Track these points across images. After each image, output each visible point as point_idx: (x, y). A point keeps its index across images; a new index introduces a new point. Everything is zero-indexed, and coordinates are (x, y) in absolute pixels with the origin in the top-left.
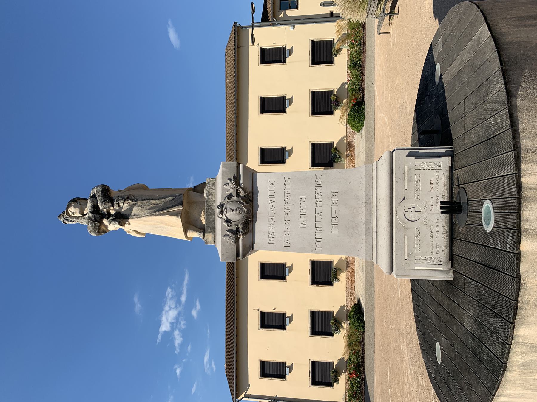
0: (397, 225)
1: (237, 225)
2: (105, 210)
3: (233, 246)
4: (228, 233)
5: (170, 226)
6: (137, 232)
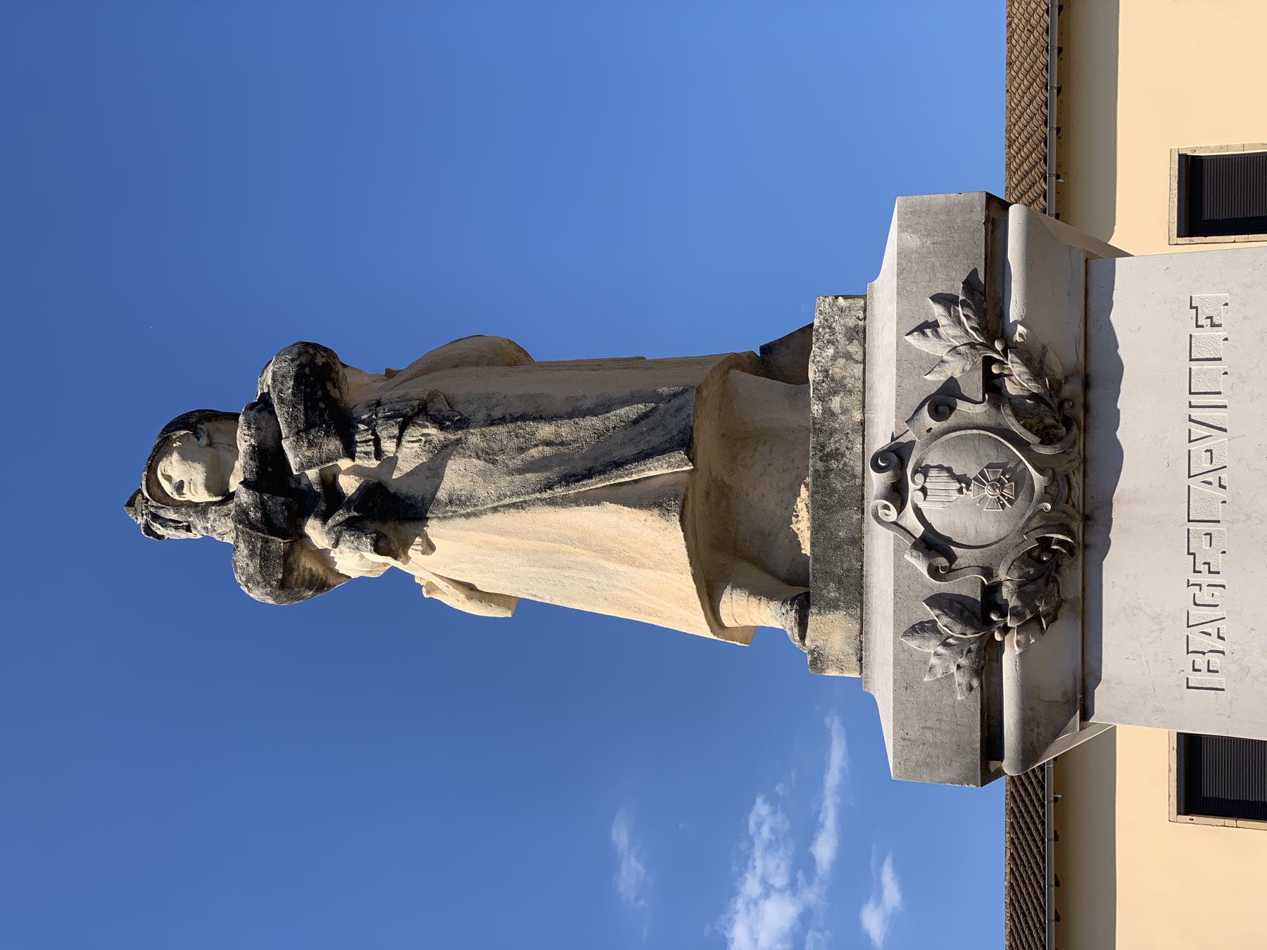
1: (988, 572)
2: (312, 474)
3: (962, 697)
4: (932, 614)
5: (625, 563)
6: (469, 589)
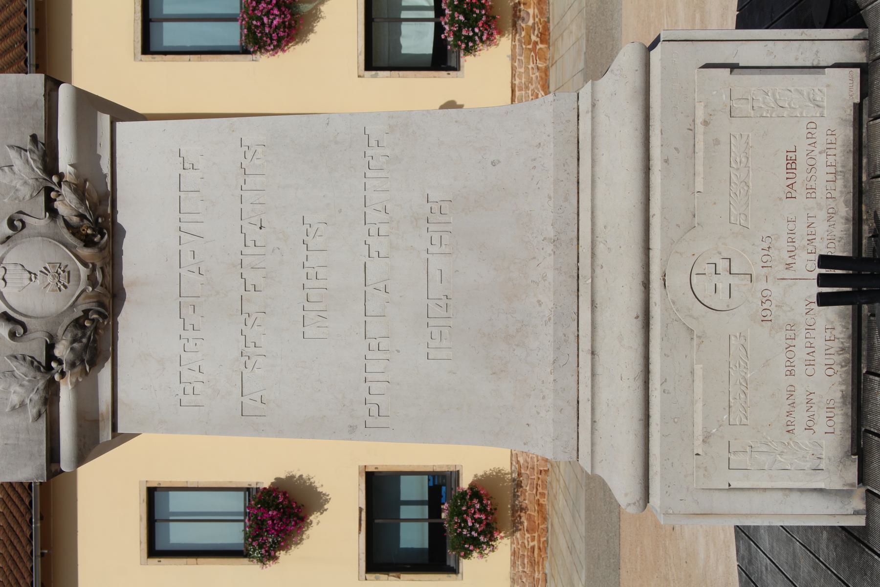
0: (666, 326)
